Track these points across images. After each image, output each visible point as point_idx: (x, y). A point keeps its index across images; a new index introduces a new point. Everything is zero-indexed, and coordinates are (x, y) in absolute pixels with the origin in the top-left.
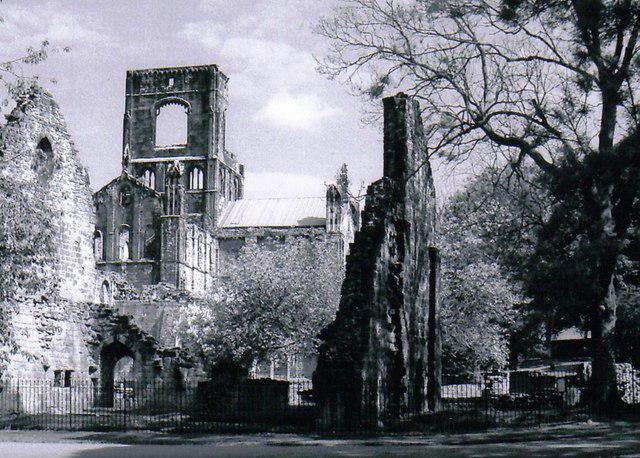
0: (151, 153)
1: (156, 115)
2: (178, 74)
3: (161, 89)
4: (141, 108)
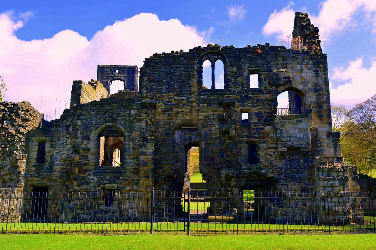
1: (110, 85)
2: (121, 68)
3: (113, 74)
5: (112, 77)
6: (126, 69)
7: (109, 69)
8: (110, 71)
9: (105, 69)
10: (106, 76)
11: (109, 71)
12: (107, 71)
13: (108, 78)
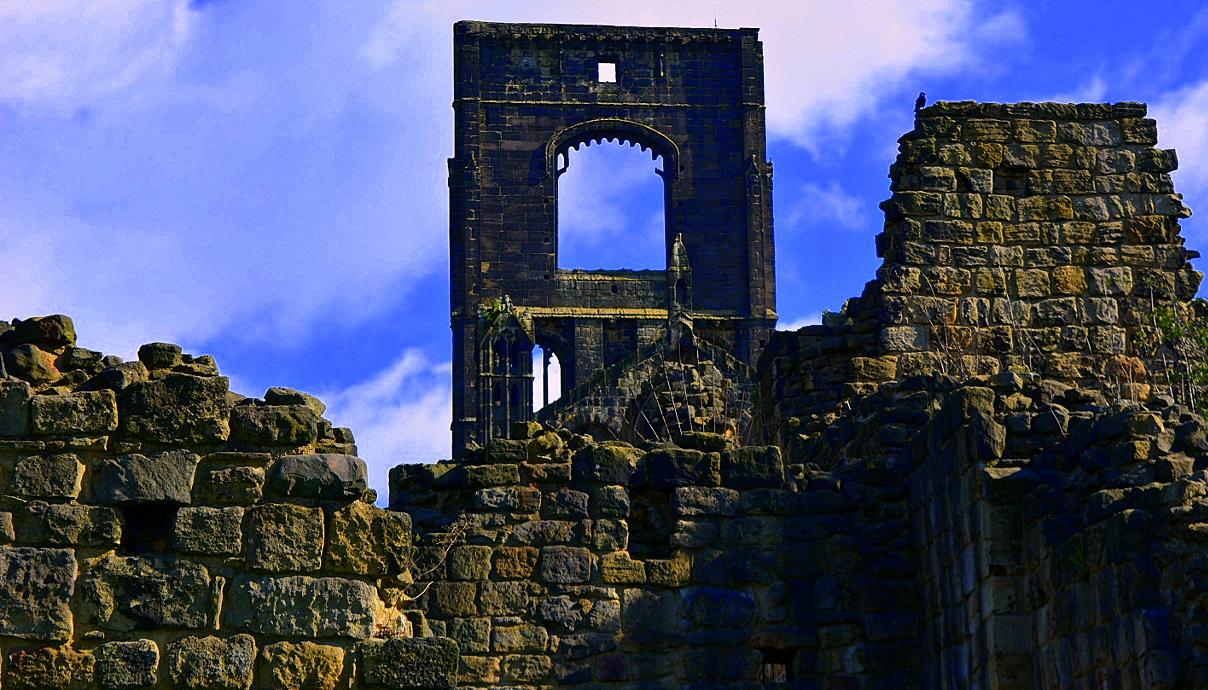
0: (544, 288)
2: (635, 47)
3: (574, 91)
4: (509, 145)
5: (571, 114)
6: (671, 59)
7: (544, 57)
8: (554, 71)
9: (516, 51)
10: (524, 110)
11: (545, 72)
12: (531, 73)
13: (544, 121)
